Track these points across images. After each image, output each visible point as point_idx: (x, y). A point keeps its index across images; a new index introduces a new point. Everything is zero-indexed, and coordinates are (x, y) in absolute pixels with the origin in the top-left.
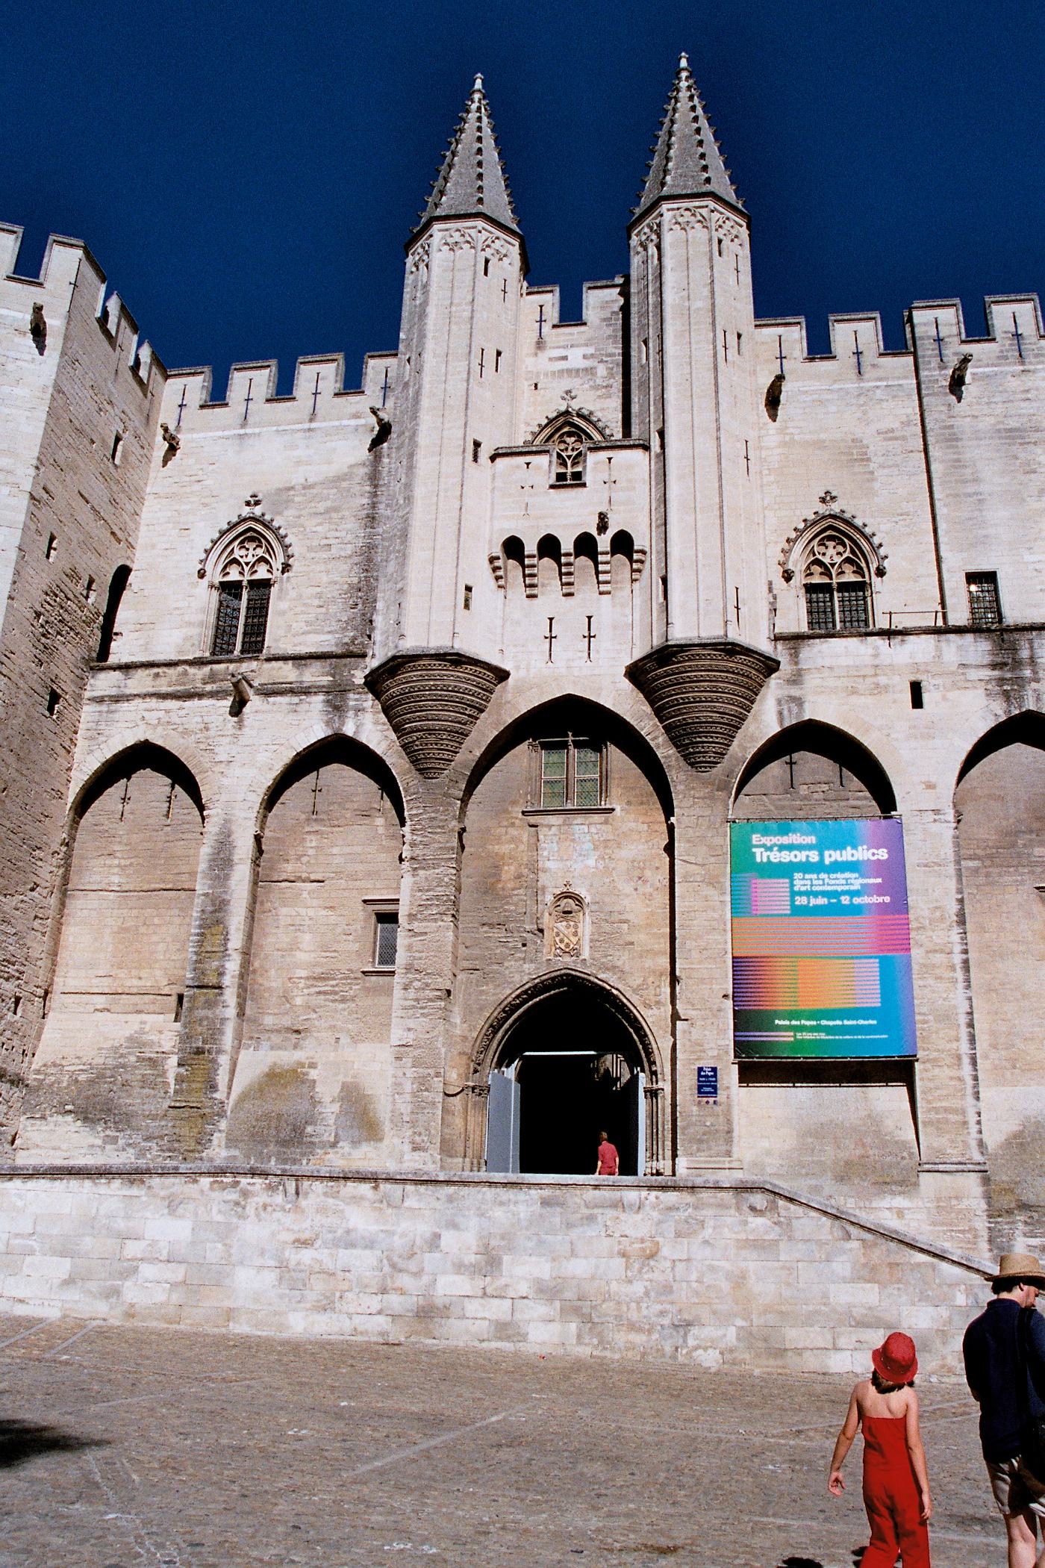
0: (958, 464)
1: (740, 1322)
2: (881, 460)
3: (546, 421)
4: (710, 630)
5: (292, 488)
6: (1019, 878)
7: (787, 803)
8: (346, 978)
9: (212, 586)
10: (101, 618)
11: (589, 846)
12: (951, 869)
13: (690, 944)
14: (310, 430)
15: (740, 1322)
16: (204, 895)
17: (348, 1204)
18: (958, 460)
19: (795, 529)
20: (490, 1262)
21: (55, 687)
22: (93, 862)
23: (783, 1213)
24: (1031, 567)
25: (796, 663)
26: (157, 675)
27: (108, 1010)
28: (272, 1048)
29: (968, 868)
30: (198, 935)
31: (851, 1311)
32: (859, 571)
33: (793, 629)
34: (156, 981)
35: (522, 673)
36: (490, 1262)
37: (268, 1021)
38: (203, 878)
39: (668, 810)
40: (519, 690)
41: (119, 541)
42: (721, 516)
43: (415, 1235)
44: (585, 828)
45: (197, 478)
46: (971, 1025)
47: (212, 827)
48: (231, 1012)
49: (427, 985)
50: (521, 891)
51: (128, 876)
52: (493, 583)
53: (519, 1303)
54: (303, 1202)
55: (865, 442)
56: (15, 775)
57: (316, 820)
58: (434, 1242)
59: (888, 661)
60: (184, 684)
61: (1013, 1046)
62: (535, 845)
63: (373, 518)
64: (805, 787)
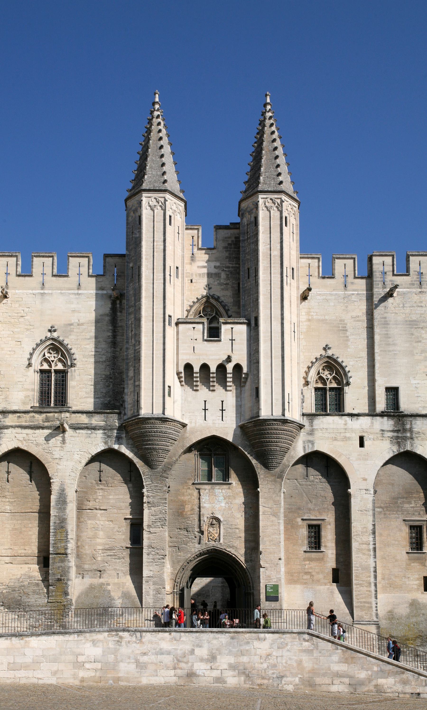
1: (300, 676)
6: (397, 516)
12: (371, 513)
16: (54, 516)
20: (212, 658)
36: (212, 658)
38: (54, 509)
43: (185, 650)
44: (220, 490)
57: (101, 484)
58: (192, 652)
64: (313, 476)
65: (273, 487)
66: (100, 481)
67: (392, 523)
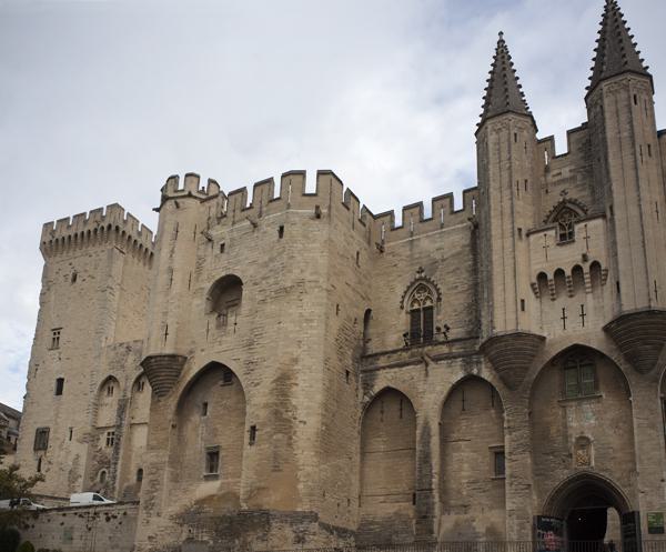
9: (407, 313)
11: (591, 414)
13: (643, 457)
47: (420, 422)
48: (437, 499)
52: (533, 296)
62: (565, 417)
66: (464, 410)
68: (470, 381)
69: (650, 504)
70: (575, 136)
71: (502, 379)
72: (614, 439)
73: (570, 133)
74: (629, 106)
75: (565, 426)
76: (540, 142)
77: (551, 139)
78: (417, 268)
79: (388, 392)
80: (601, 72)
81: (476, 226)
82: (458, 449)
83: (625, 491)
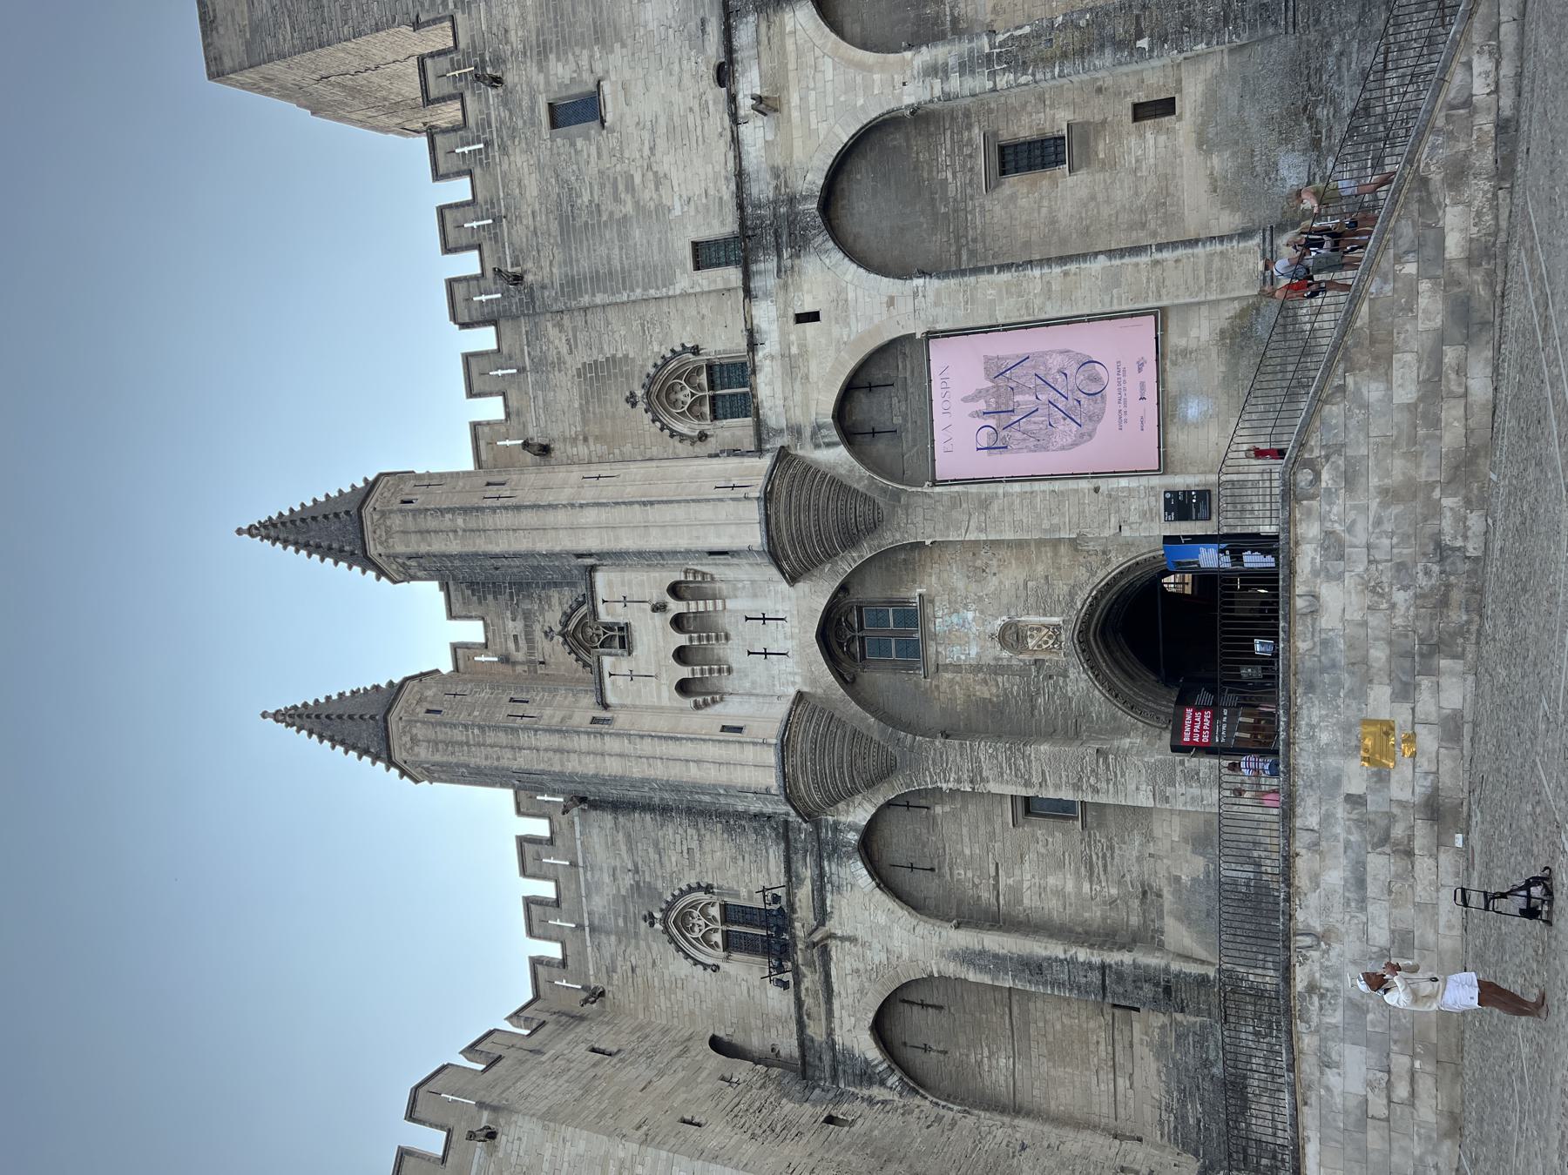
0: (598, 280)
2: (595, 351)
3: (573, 655)
4: (754, 512)
5: (638, 883)
7: (910, 436)
8: (1090, 846)
9: (727, 958)
10: (759, 1067)
11: (955, 619)
13: (1046, 525)
14: (585, 868)
15: (1437, 494)
17: (1318, 886)
18: (592, 278)
19: (662, 429)
21: (822, 1119)
22: (988, 1083)
23: (1316, 453)
24: (686, 209)
25: (782, 431)
26: (809, 1016)
27: (1131, 1075)
28: (1162, 918)
29: (969, 260)
30: (1052, 988)
31: (1424, 381)
32: (698, 370)
33: (751, 432)
34: (1100, 1027)
35: (798, 679)
37: (1134, 920)
39: (920, 545)
40: (814, 681)
41: (686, 1051)
42: (652, 503)
43: (1349, 819)
44: (938, 621)
45: (630, 974)
46: (1122, 252)
47: (952, 969)
48: (1126, 958)
49: (1093, 771)
50: (1000, 679)
51: (999, 1049)
52: (718, 707)
53: (1420, 715)
54: (1319, 929)
55: (580, 366)
56: (905, 1165)
59: (778, 347)
60: (816, 992)
61: (1142, 207)
62: (957, 668)
63: (663, 809)
65: (920, 510)
66: (932, 870)
67: (996, 220)
68: (869, 847)
69: (1146, 515)
70: (456, 608)
71: (870, 785)
72: (1008, 577)
73: (451, 615)
74: (416, 512)
75: (977, 668)
76: (457, 669)
77: (455, 648)
78: (644, 925)
79: (879, 1028)
80: (352, 553)
81: (583, 800)
82: (1016, 891)
83: (1118, 561)
